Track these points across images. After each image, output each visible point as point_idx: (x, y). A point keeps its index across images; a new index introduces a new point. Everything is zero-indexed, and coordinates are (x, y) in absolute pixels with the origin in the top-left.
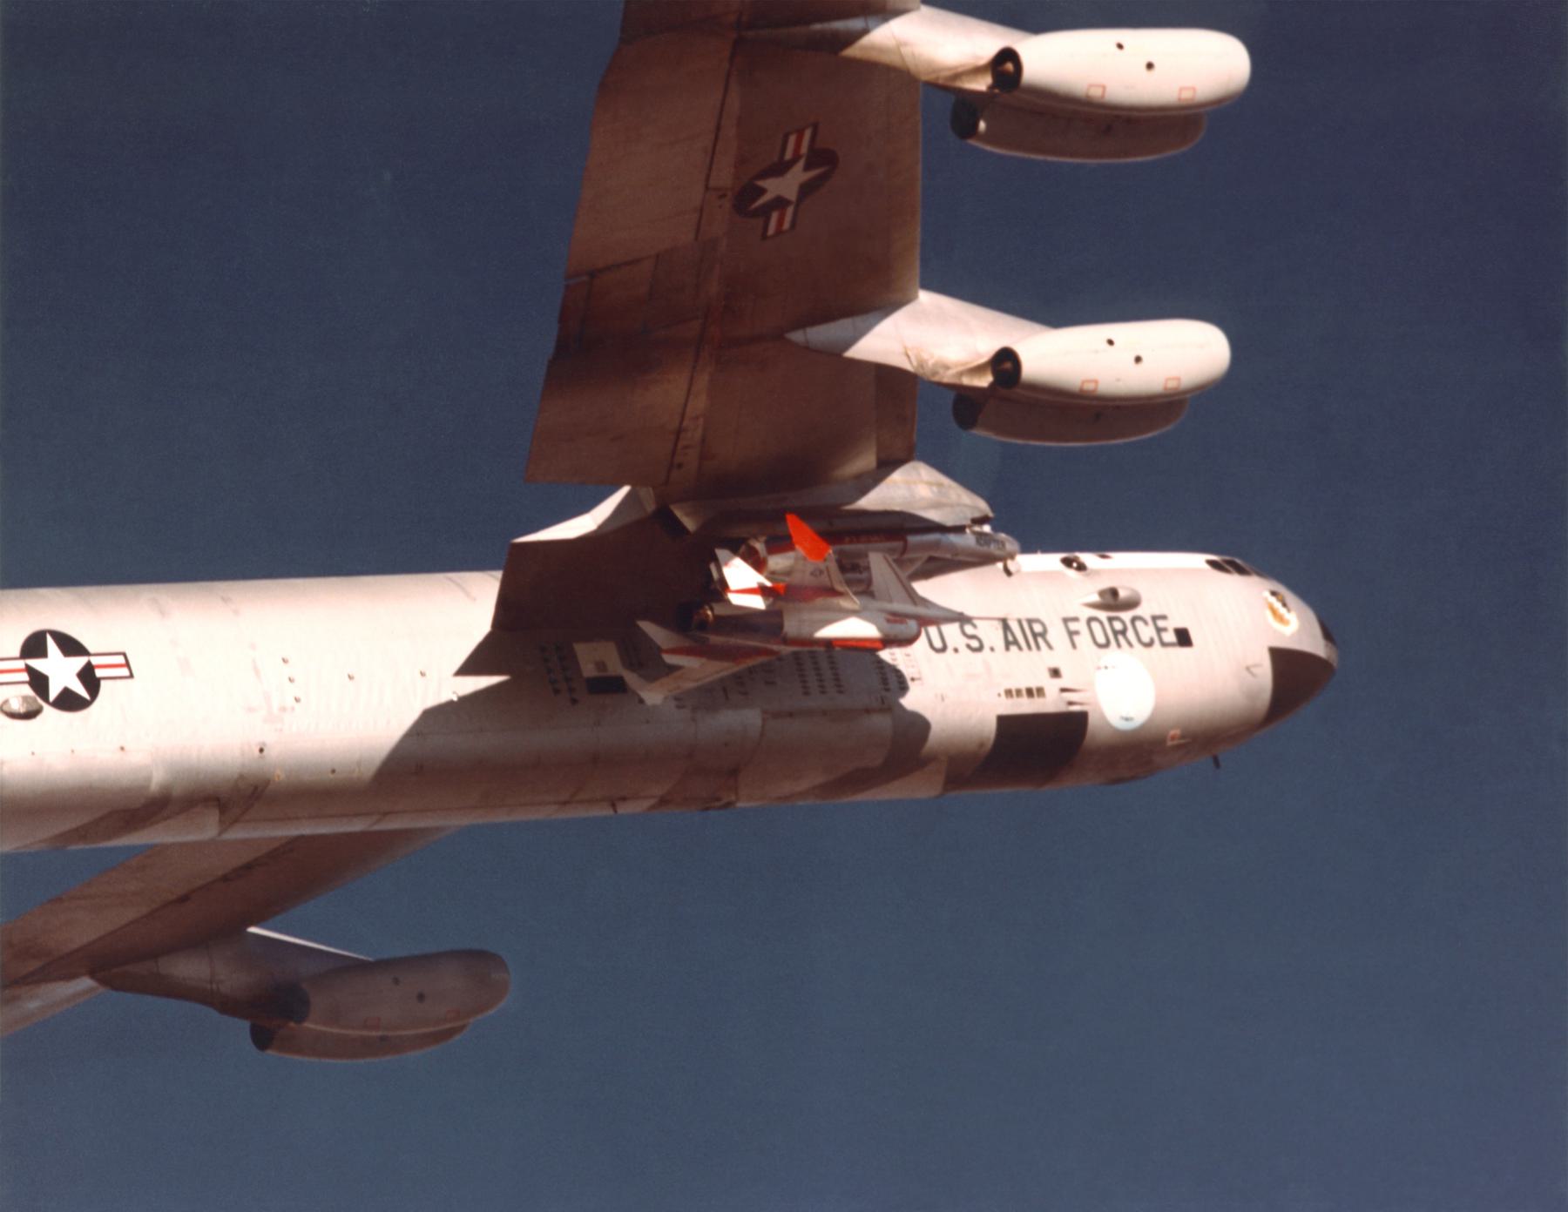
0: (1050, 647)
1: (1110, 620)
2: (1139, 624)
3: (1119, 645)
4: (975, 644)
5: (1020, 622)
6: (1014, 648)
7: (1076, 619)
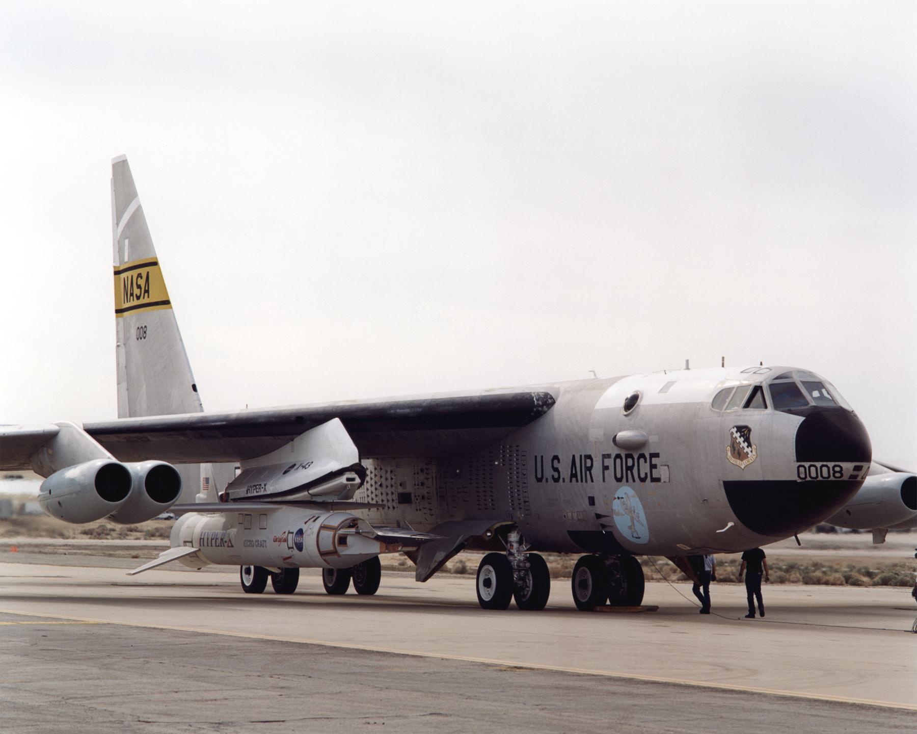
0: (592, 481)
1: (628, 456)
2: (642, 460)
3: (627, 481)
4: (556, 476)
5: (581, 456)
6: (574, 479)
7: (609, 456)
